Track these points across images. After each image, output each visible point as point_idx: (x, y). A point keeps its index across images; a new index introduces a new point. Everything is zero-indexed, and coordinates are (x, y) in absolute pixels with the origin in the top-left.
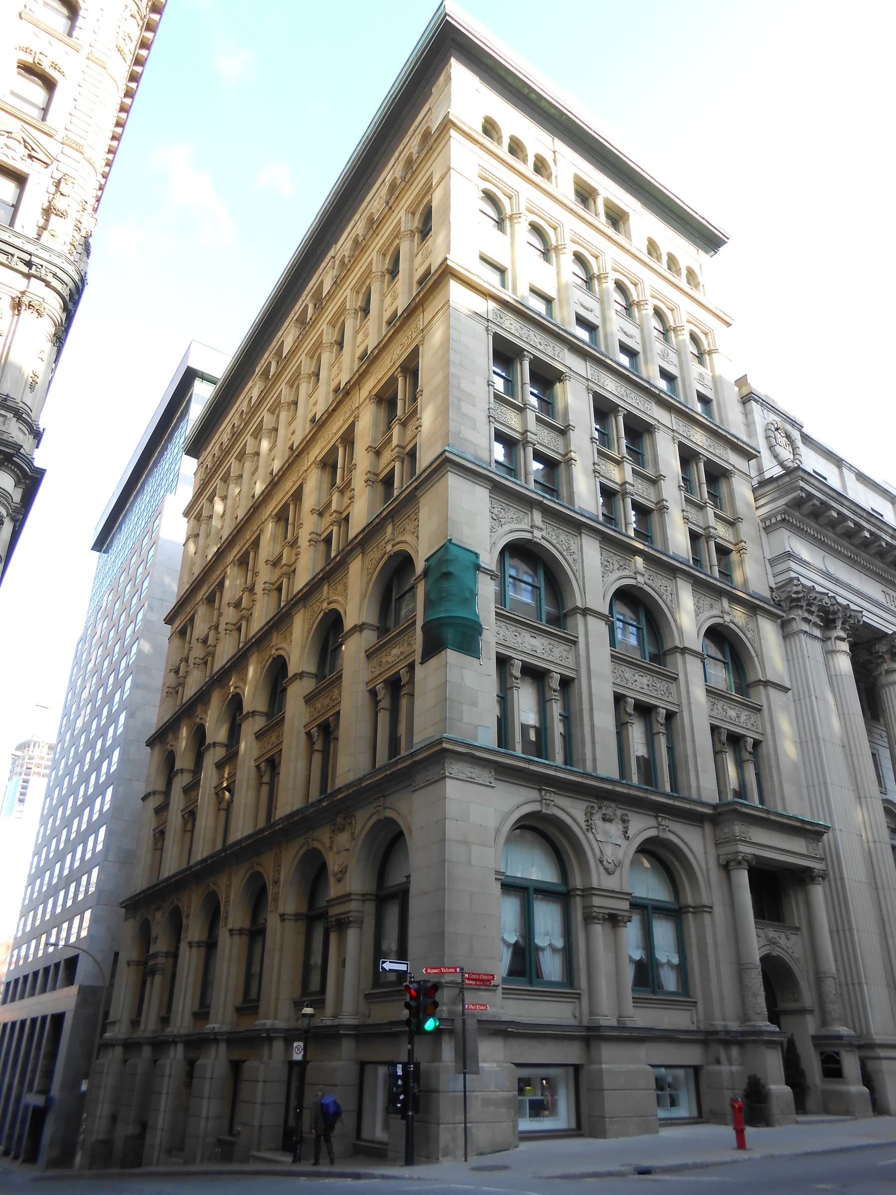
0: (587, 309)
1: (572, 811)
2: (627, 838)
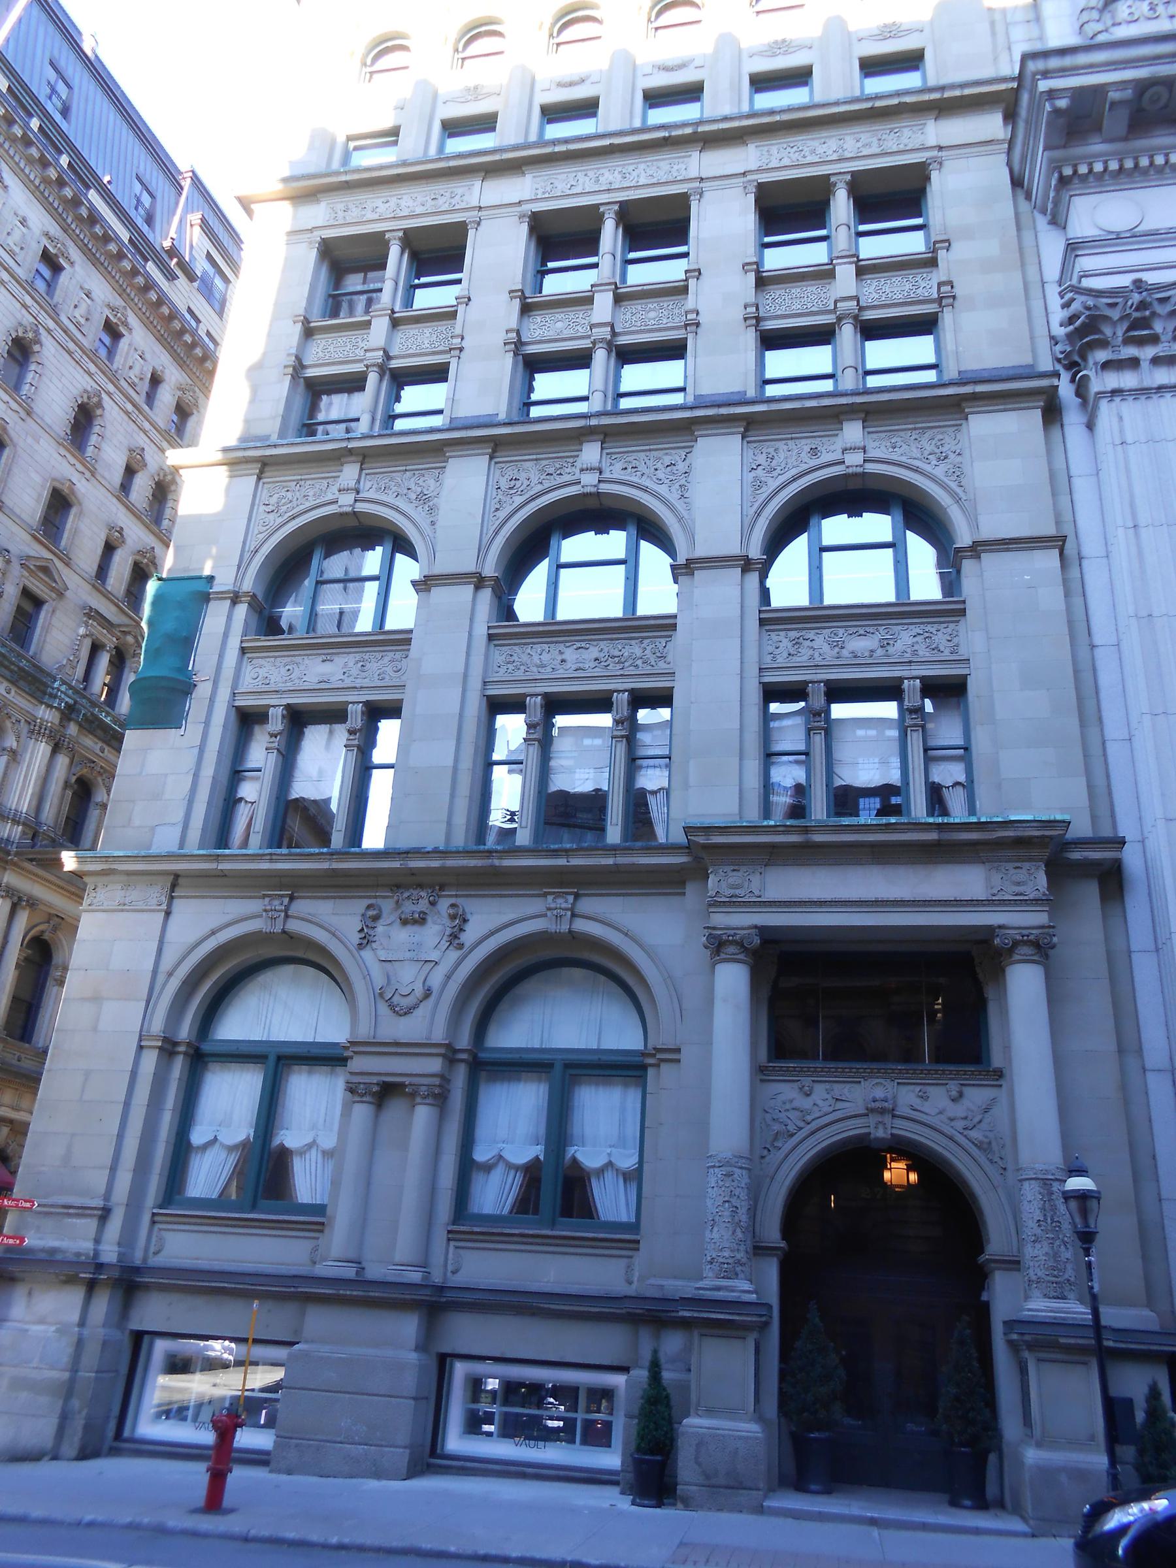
0: (571, 84)
2: (461, 946)
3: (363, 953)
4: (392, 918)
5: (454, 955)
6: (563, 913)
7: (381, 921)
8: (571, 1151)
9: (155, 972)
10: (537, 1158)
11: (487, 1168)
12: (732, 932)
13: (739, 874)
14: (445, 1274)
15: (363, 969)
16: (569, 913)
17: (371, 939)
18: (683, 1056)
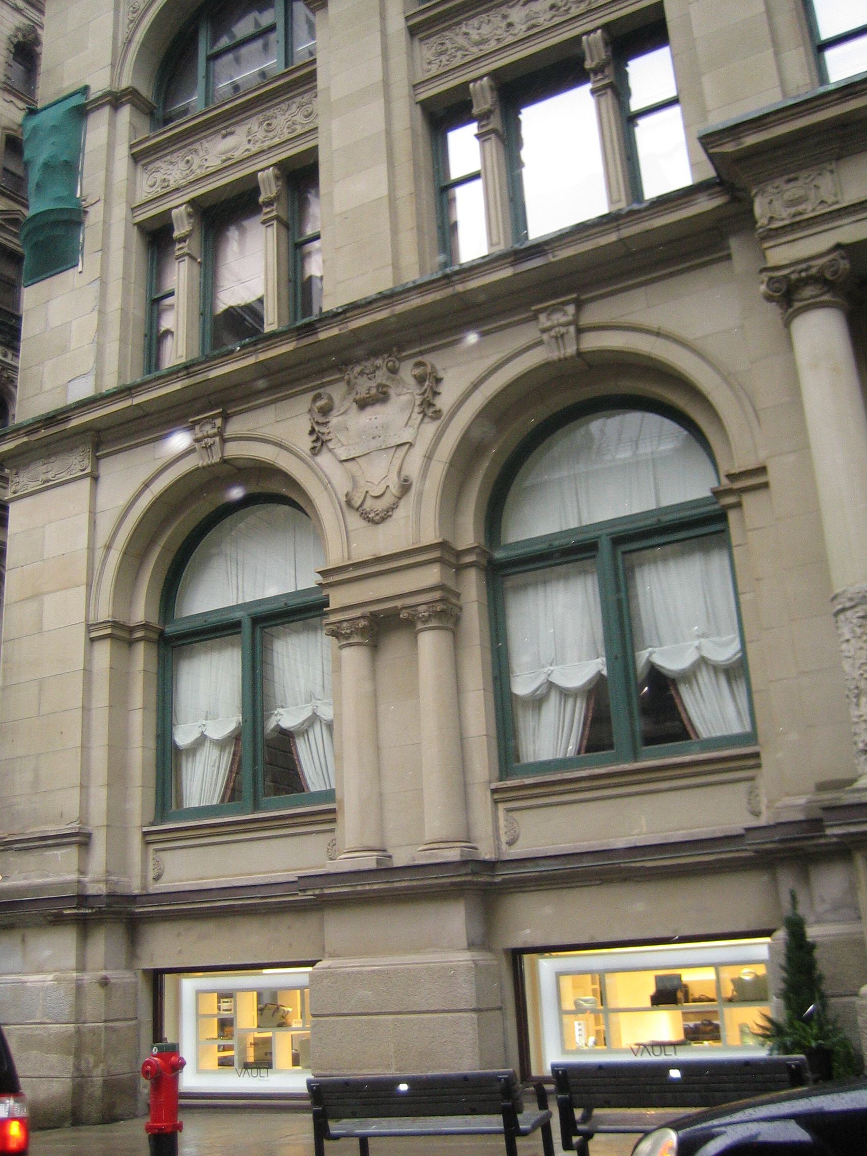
1: (275, 433)
2: (437, 414)
3: (319, 459)
4: (347, 404)
5: (430, 428)
6: (563, 330)
7: (335, 412)
8: (643, 657)
9: (91, 549)
10: (599, 675)
11: (537, 702)
12: (804, 266)
13: (799, 183)
14: (499, 848)
15: (324, 480)
16: (572, 329)
17: (325, 438)
18: (772, 476)
